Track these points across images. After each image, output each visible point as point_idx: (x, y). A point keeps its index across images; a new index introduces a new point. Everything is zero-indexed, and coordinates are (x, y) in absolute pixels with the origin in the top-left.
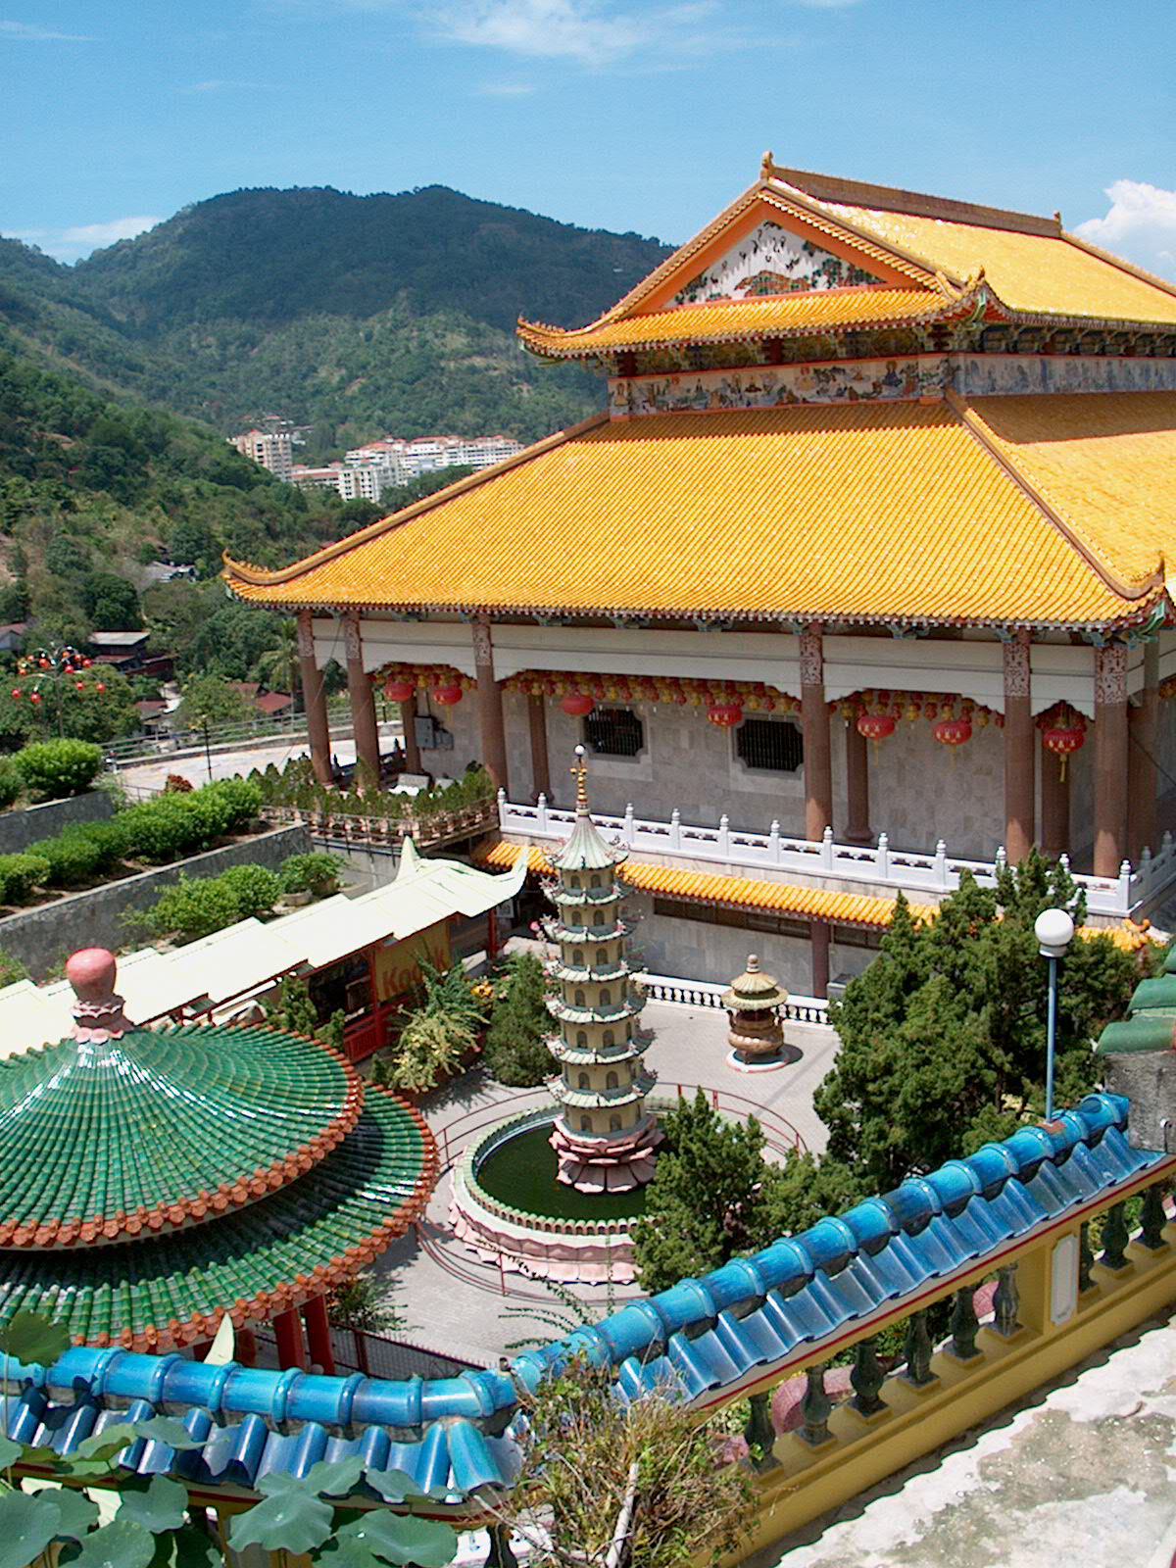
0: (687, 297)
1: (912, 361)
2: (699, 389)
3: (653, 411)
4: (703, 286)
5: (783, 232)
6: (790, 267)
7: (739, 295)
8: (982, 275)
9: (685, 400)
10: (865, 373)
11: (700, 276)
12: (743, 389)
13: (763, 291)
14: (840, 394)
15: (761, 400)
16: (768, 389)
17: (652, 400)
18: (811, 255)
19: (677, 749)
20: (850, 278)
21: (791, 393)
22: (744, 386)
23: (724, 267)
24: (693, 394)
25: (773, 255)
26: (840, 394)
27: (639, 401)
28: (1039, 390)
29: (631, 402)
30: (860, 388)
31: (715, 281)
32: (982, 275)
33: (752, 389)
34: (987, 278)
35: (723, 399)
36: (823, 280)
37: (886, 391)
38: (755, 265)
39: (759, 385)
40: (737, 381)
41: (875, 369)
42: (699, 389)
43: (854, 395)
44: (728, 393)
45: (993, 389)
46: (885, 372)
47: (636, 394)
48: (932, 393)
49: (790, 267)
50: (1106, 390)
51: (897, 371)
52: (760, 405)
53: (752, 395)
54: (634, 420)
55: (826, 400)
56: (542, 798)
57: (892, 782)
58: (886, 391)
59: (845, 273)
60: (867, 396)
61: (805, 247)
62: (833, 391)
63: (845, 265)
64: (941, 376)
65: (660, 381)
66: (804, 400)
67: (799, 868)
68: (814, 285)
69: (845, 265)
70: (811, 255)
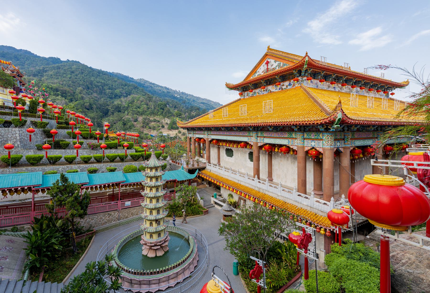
8: (307, 54)
14: (280, 89)
17: (247, 95)
26: (280, 89)
32: (307, 54)
35: (259, 93)
37: (289, 87)
55: (277, 91)
58: (289, 87)
59: (282, 65)
60: (285, 89)
62: (278, 89)
69: (282, 63)
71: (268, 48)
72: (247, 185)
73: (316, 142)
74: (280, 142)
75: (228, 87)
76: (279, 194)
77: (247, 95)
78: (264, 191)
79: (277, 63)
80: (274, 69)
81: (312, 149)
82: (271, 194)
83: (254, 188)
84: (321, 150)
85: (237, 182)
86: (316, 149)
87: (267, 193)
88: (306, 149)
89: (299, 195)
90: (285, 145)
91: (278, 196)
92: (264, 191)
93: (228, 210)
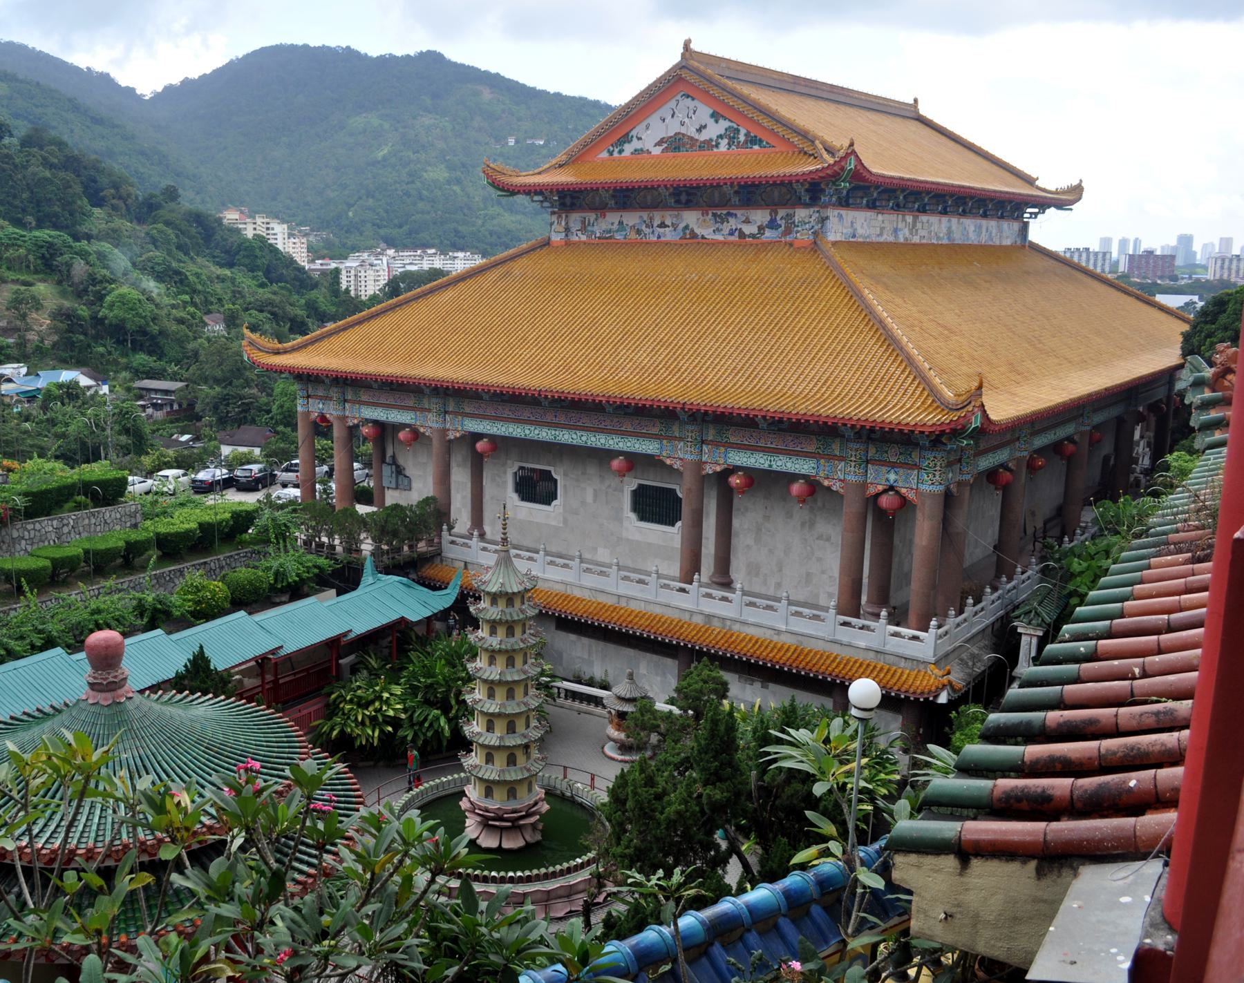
0: (617, 150)
1: (790, 211)
2: (621, 223)
3: (584, 238)
4: (629, 142)
5: (696, 103)
6: (699, 130)
7: (657, 151)
8: (852, 145)
9: (610, 231)
10: (752, 218)
11: (627, 134)
12: (655, 224)
13: (677, 149)
14: (731, 233)
15: (669, 235)
16: (675, 226)
17: (583, 229)
18: (717, 122)
19: (583, 503)
20: (746, 142)
21: (692, 231)
22: (657, 222)
23: (647, 128)
24: (615, 227)
25: (686, 120)
26: (731, 233)
27: (573, 230)
28: (891, 239)
29: (567, 230)
30: (747, 229)
31: (639, 139)
32: (852, 145)
33: (663, 225)
34: (856, 147)
35: (639, 232)
36: (724, 142)
38: (673, 128)
39: (668, 222)
40: (651, 219)
41: (760, 216)
42: (621, 223)
43: (742, 235)
44: (644, 228)
45: (854, 236)
46: (769, 218)
47: (571, 225)
48: (803, 236)
49: (699, 130)
50: (945, 242)
51: (778, 218)
52: (668, 238)
53: (662, 230)
54: (568, 243)
55: (719, 237)
56: (476, 533)
57: (750, 540)
58: (769, 234)
59: (742, 138)
60: (753, 236)
61: (712, 116)
62: (726, 231)
63: (743, 131)
64: (813, 223)
65: (591, 216)
66: (703, 237)
67: (675, 603)
68: (717, 146)
69: (743, 131)
70: (717, 122)
71: (687, 44)
72: (658, 610)
73: (901, 471)
74: (789, 465)
75: (495, 185)
76: (783, 628)
77: (583, 229)
78: (728, 623)
79: (724, 125)
80: (709, 145)
81: (885, 491)
82: (751, 631)
83: (686, 617)
84: (911, 496)
85: (610, 601)
86: (897, 492)
87: (736, 627)
88: (872, 490)
89: (845, 624)
90: (804, 476)
91: (779, 632)
92: (728, 623)
93: (628, 696)
